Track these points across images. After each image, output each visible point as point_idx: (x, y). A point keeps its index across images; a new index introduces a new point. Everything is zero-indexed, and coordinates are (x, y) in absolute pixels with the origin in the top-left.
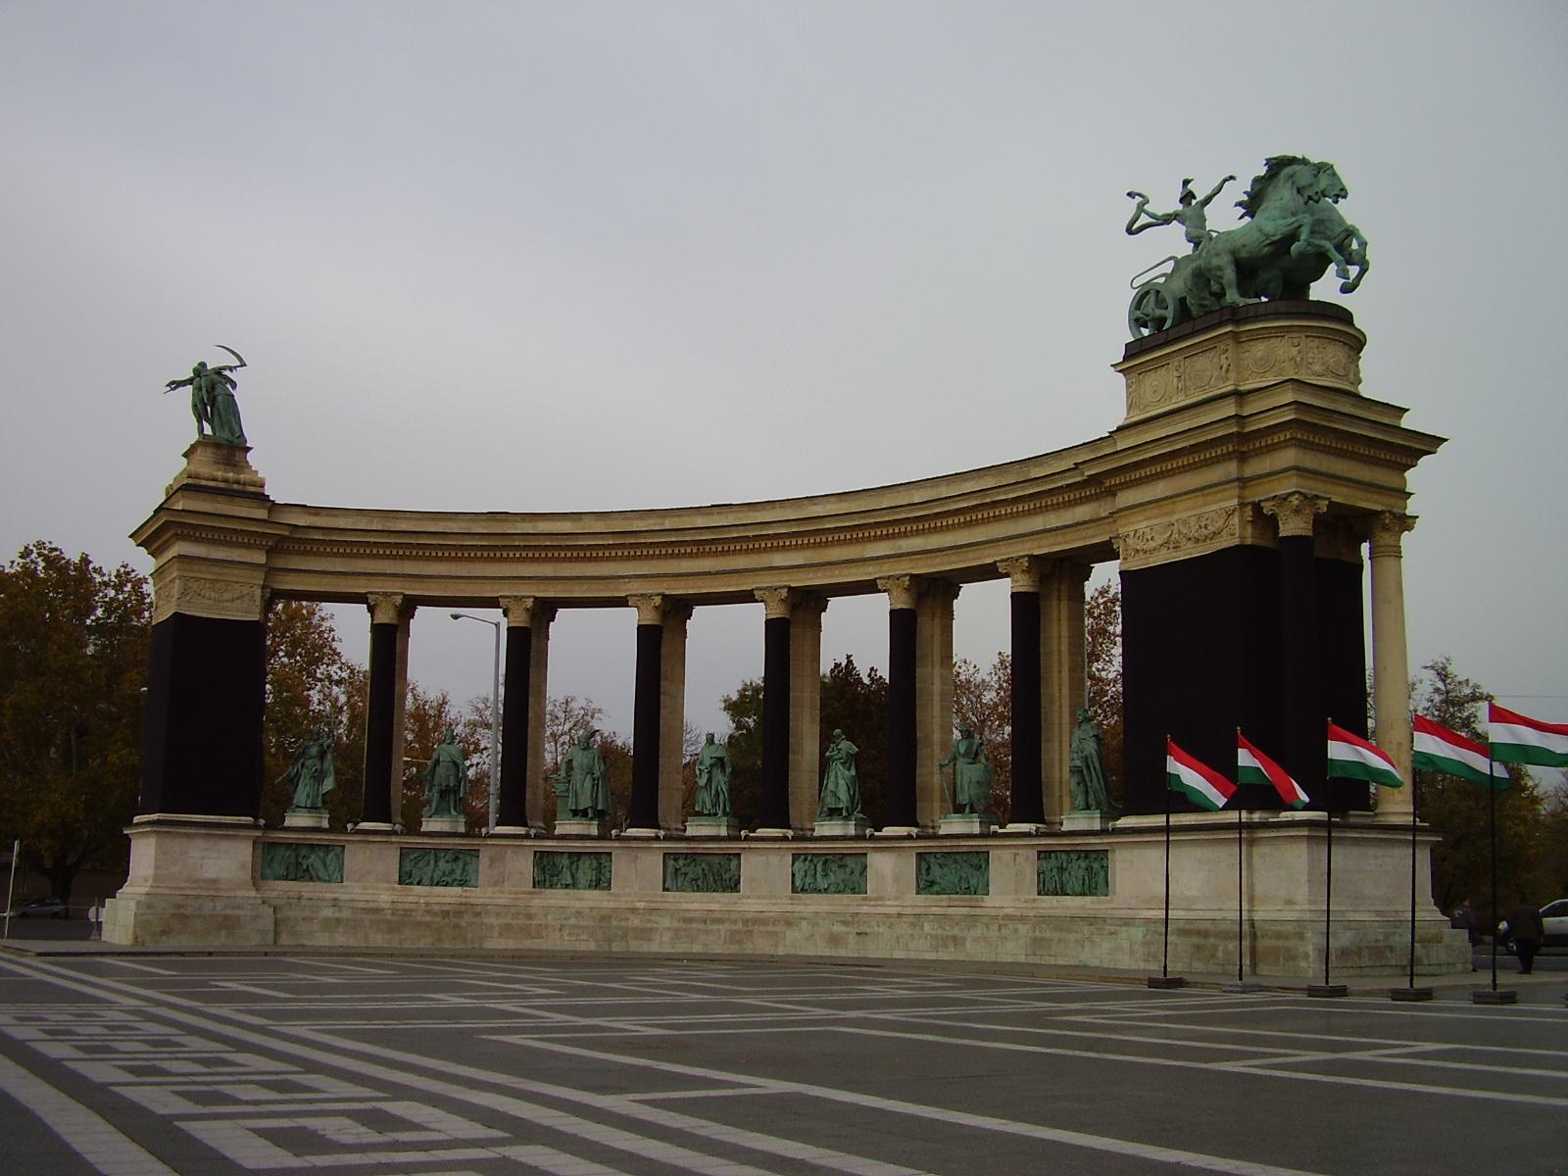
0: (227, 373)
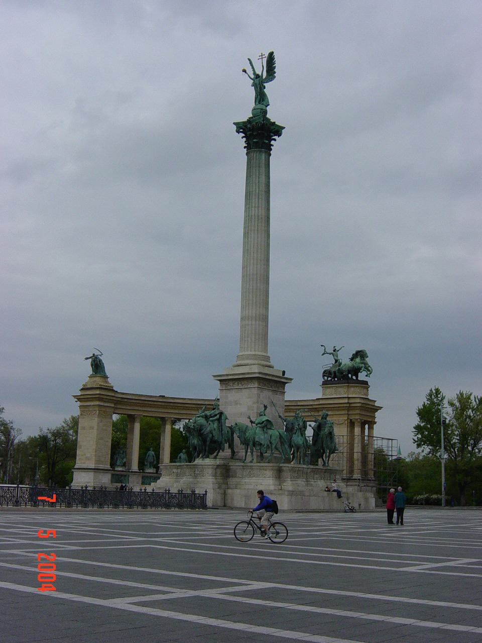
0: (99, 356)
